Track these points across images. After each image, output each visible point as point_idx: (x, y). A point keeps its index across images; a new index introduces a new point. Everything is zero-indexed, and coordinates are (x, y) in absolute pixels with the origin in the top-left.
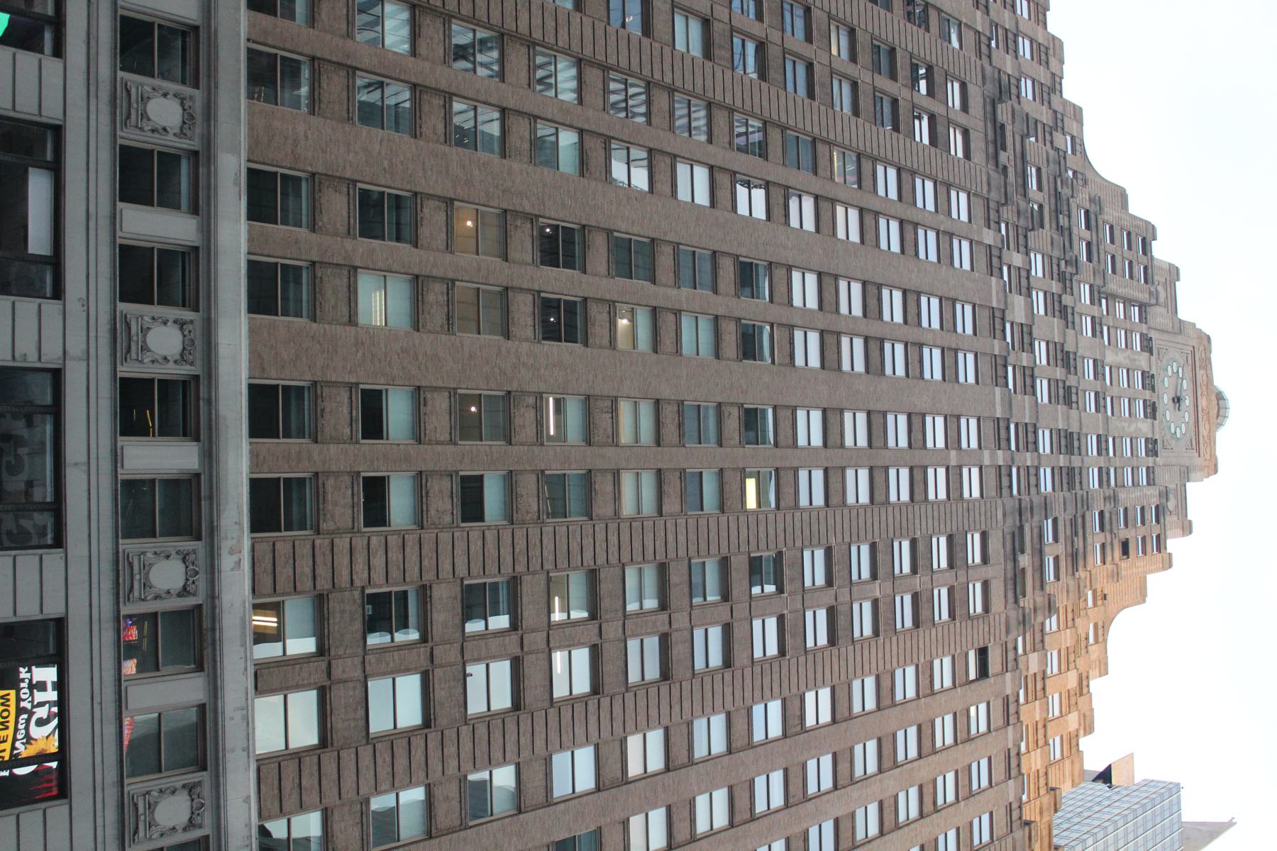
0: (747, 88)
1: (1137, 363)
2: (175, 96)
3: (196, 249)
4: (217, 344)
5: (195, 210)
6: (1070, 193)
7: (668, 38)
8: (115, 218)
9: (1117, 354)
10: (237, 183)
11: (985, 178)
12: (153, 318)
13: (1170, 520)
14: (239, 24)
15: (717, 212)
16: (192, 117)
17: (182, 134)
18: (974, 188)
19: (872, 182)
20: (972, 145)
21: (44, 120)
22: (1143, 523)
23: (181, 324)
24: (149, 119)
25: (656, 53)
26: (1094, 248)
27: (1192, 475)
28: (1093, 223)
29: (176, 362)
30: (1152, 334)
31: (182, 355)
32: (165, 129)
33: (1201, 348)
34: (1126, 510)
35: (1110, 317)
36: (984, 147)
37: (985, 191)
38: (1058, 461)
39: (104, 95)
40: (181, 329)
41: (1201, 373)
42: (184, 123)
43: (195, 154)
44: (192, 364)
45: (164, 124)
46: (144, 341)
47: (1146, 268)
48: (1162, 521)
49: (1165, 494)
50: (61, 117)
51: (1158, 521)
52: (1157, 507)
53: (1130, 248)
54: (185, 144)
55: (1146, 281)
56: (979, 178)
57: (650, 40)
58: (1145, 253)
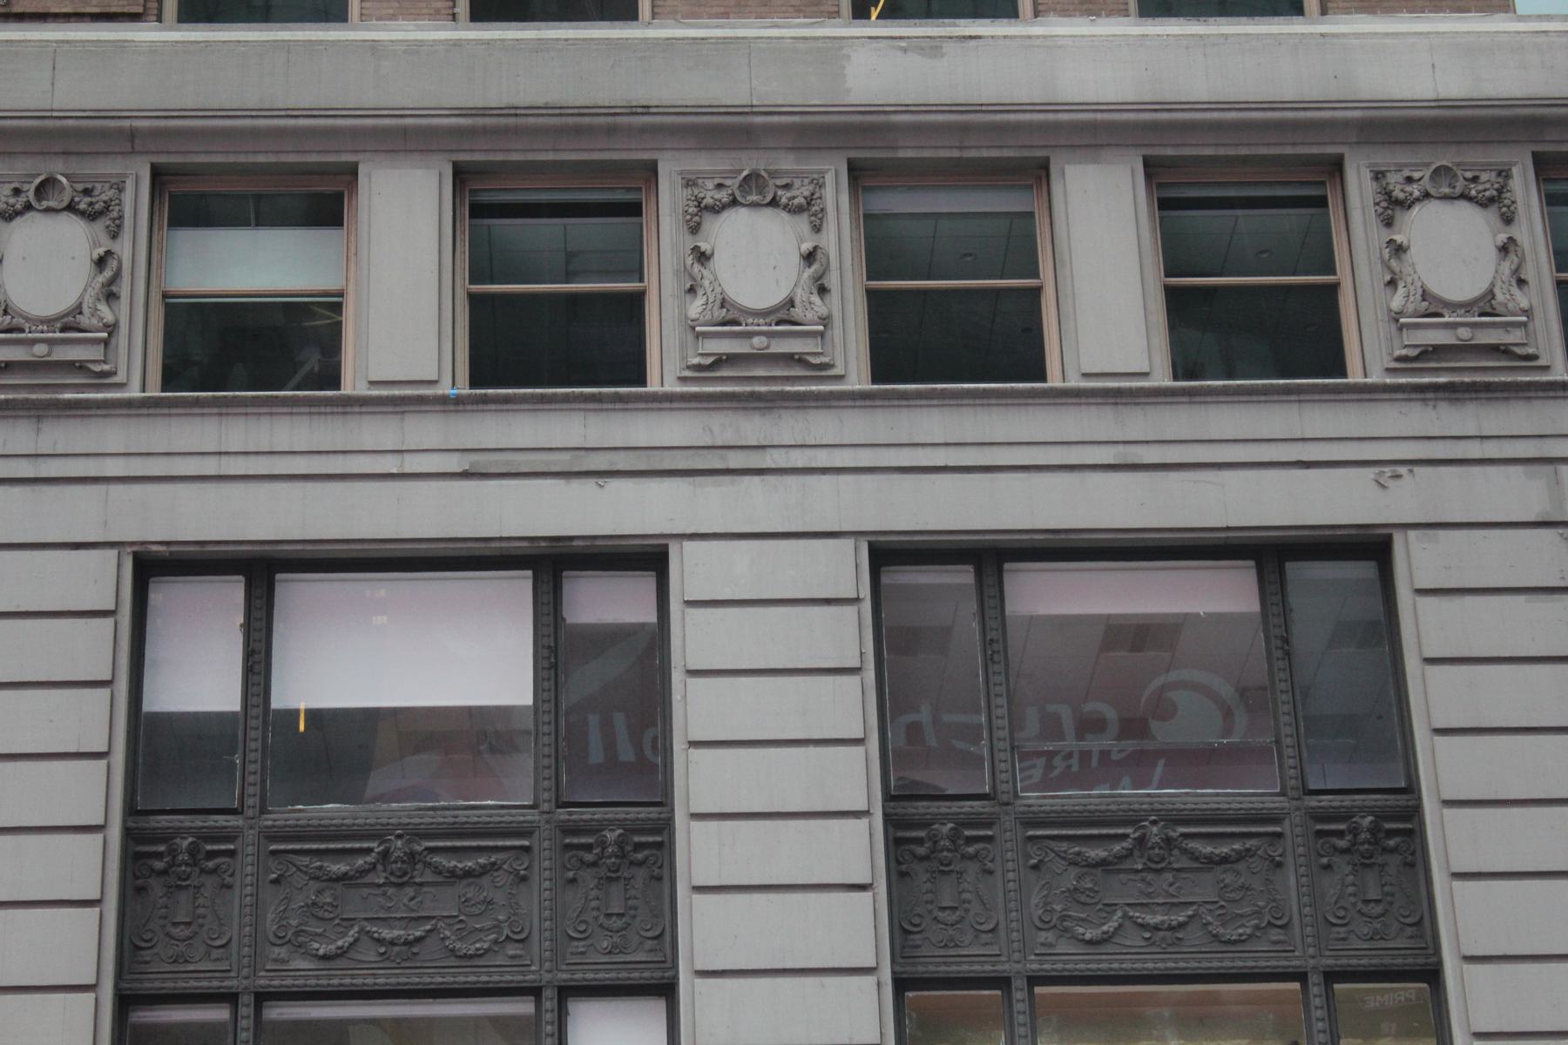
2: (695, 229)
3: (1151, 166)
4: (1440, 104)
5: (1037, 174)
8: (1119, 393)
10: (932, 48)
12: (1392, 283)
14: (420, 43)
16: (753, 181)
17: (809, 209)
21: (866, 592)
23: (1392, 206)
24: (790, 303)
29: (1508, 220)
31: (1484, 203)
32: (809, 257)
39: (753, 427)
40: (1406, 204)
42: (774, 203)
43: (858, 174)
44: (1504, 174)
45: (795, 260)
46: (1467, 306)
50: (847, 544)
54: (836, 197)
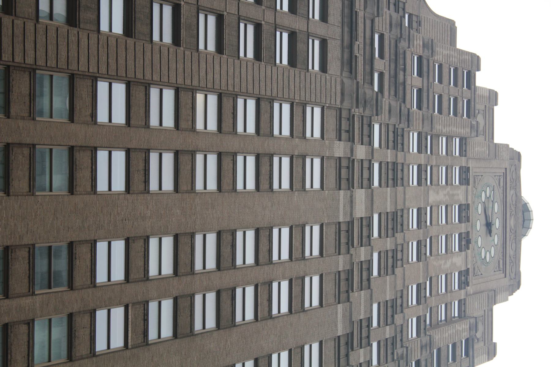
0: (112, 49)
1: (456, 198)
6: (407, 45)
7: (32, 10)
9: (438, 193)
11: (339, 88)
13: (478, 346)
15: (76, 199)
18: (328, 102)
19: (231, 122)
20: (329, 55)
22: (454, 359)
25: (18, 32)
26: (425, 95)
27: (499, 297)
28: (425, 69)
30: (471, 165)
33: (513, 168)
34: (439, 350)
35: (434, 157)
36: (340, 56)
37: (338, 102)
38: (385, 333)
41: (510, 193)
47: (469, 102)
48: (471, 353)
49: (474, 328)
51: (467, 354)
52: (467, 341)
53: (456, 84)
55: (468, 116)
56: (333, 90)
57: (12, 18)
58: (469, 87)
